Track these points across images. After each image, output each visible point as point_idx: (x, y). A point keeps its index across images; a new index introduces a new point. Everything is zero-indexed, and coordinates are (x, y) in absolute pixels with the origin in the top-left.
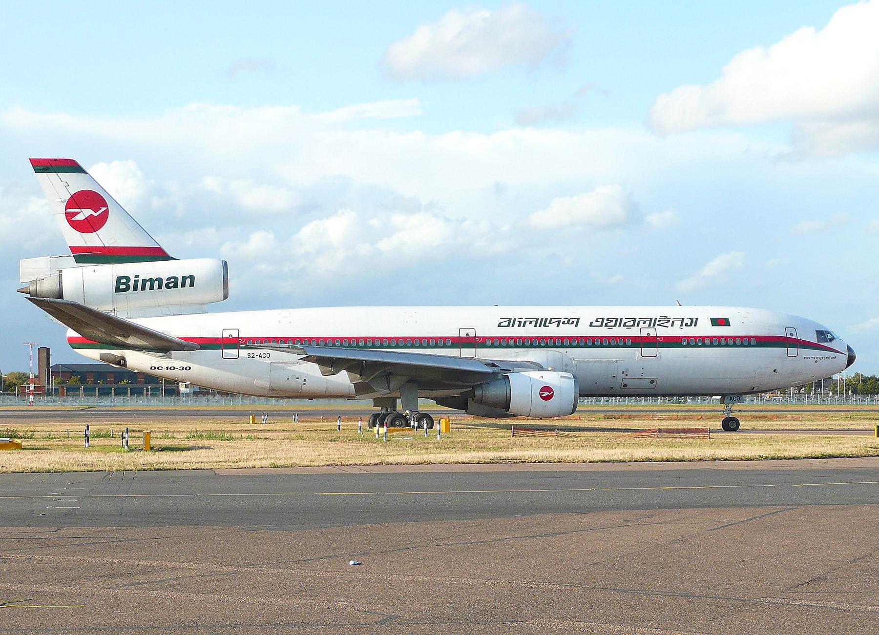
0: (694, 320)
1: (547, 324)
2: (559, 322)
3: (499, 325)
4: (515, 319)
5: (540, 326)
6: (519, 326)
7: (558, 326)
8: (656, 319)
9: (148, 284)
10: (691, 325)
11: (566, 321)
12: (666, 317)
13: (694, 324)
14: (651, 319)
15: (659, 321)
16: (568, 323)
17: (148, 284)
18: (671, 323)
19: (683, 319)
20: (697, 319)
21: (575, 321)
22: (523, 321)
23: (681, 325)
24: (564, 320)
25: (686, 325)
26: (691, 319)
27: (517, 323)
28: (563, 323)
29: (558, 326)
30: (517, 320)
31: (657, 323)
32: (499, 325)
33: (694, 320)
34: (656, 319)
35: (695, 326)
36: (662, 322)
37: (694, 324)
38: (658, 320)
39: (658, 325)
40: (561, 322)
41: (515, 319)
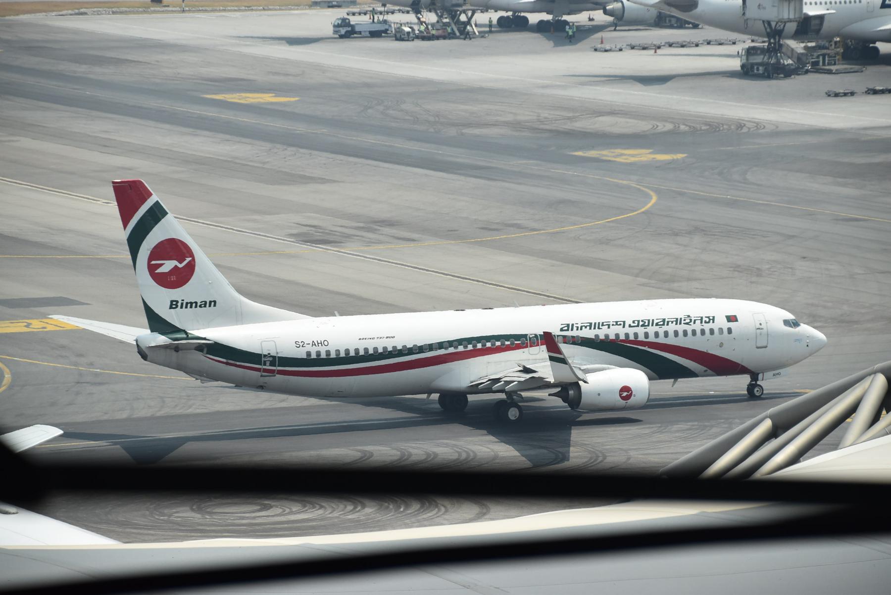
0: (711, 318)
1: (601, 327)
2: (609, 325)
3: (562, 330)
4: (573, 325)
5: (595, 328)
6: (578, 327)
7: (609, 328)
8: (681, 319)
9: (189, 305)
10: (709, 322)
11: (615, 323)
12: (689, 316)
13: (711, 321)
14: (677, 319)
15: (685, 320)
16: (617, 324)
17: (189, 305)
18: (693, 321)
19: (702, 318)
20: (714, 317)
21: (622, 323)
22: (579, 326)
23: (701, 323)
24: (613, 323)
25: (706, 322)
26: (708, 317)
27: (575, 328)
28: (613, 325)
29: (609, 328)
30: (574, 327)
31: (683, 322)
32: (562, 330)
33: (711, 318)
34: (681, 319)
35: (713, 322)
36: (688, 321)
37: (711, 321)
38: (683, 320)
39: (684, 323)
40: (611, 326)
41: (573, 325)
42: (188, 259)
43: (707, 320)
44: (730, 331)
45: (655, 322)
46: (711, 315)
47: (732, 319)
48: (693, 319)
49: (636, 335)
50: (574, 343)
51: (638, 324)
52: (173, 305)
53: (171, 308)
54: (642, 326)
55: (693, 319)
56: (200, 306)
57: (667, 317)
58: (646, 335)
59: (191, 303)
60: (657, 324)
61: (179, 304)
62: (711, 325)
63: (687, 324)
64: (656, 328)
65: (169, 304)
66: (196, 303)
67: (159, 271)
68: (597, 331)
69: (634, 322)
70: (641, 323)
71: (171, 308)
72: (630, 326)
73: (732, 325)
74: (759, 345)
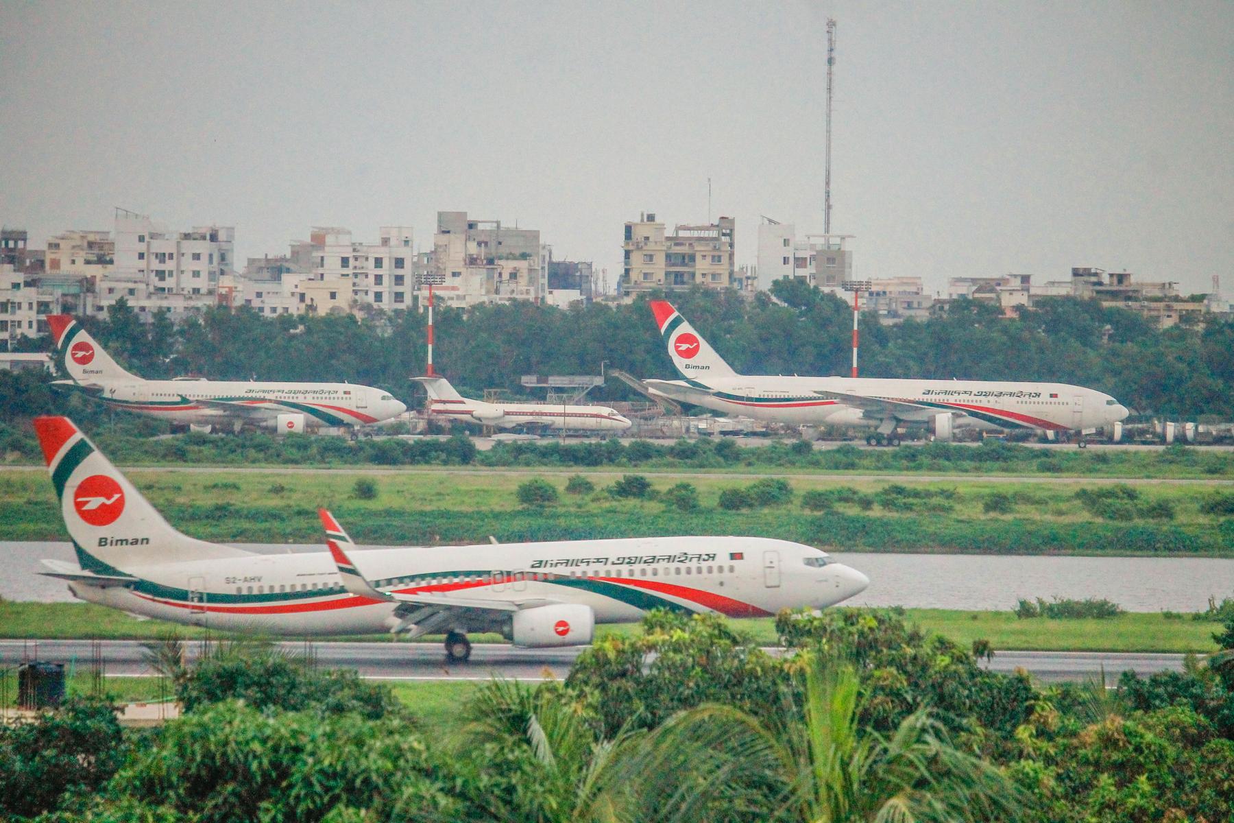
22: (554, 562)
27: (548, 565)
42: (117, 496)
43: (706, 557)
44: (732, 569)
45: (644, 559)
46: (711, 552)
47: (736, 556)
48: (690, 556)
49: (619, 572)
50: (546, 580)
51: (621, 561)
52: (102, 542)
53: (100, 545)
54: (628, 563)
55: (690, 556)
56: (132, 544)
57: (658, 554)
58: (631, 572)
59: (122, 541)
60: (645, 562)
61: (109, 541)
62: (710, 563)
63: (681, 561)
64: (643, 566)
65: (98, 541)
66: (127, 540)
67: (86, 508)
68: (574, 568)
69: (618, 559)
70: (627, 560)
71: (100, 545)
72: (613, 564)
73: (736, 563)
74: (769, 585)
